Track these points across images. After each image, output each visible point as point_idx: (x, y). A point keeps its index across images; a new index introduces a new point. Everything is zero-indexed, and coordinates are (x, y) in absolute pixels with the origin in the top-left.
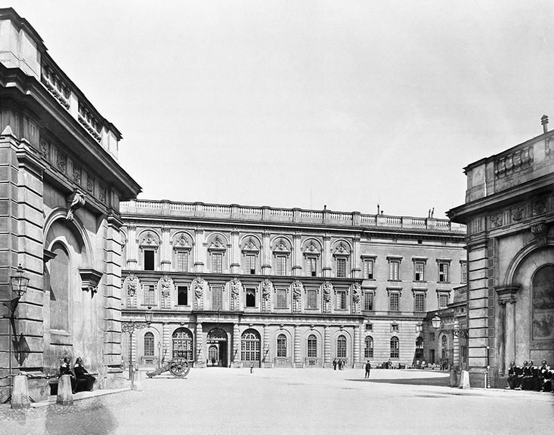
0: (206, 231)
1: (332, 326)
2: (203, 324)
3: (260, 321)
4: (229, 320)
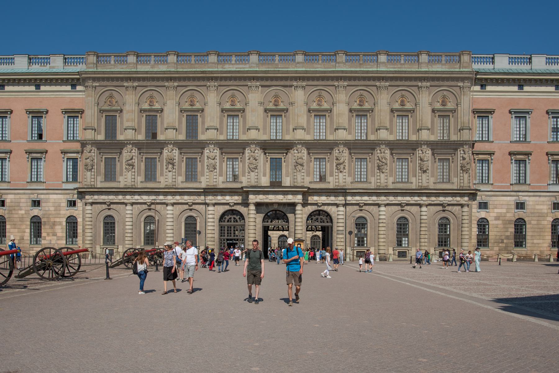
0: (262, 86)
1: (430, 205)
2: (258, 205)
3: (332, 199)
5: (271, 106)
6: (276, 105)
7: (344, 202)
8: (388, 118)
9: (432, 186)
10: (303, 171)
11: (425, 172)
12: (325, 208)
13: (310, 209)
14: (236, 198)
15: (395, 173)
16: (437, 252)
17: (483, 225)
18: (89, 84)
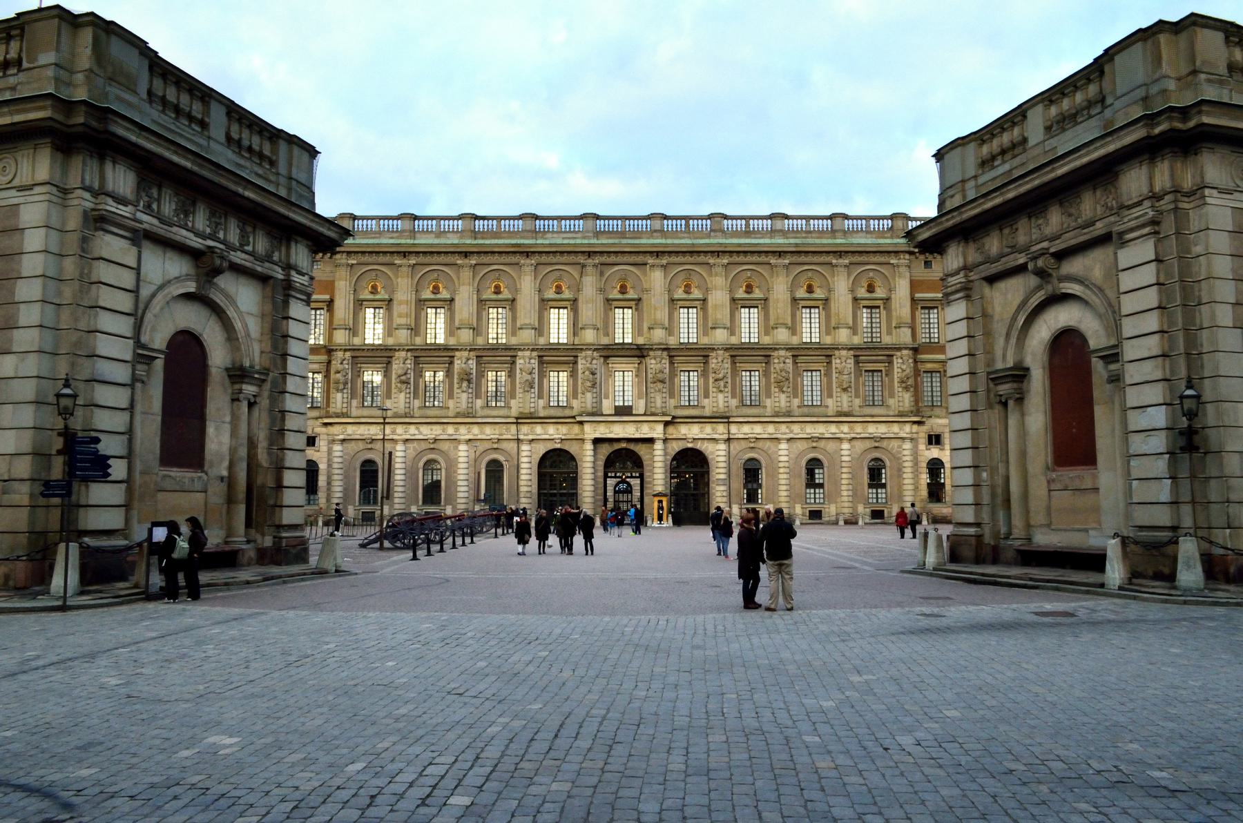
2: (597, 441)
4: (645, 431)
5: (615, 294)
7: (726, 436)
8: (789, 312)
9: (857, 410)
11: (845, 390)
12: (699, 446)
13: (676, 447)
14: (563, 429)
15: (803, 391)
16: (868, 511)
17: (935, 467)
18: (344, 261)
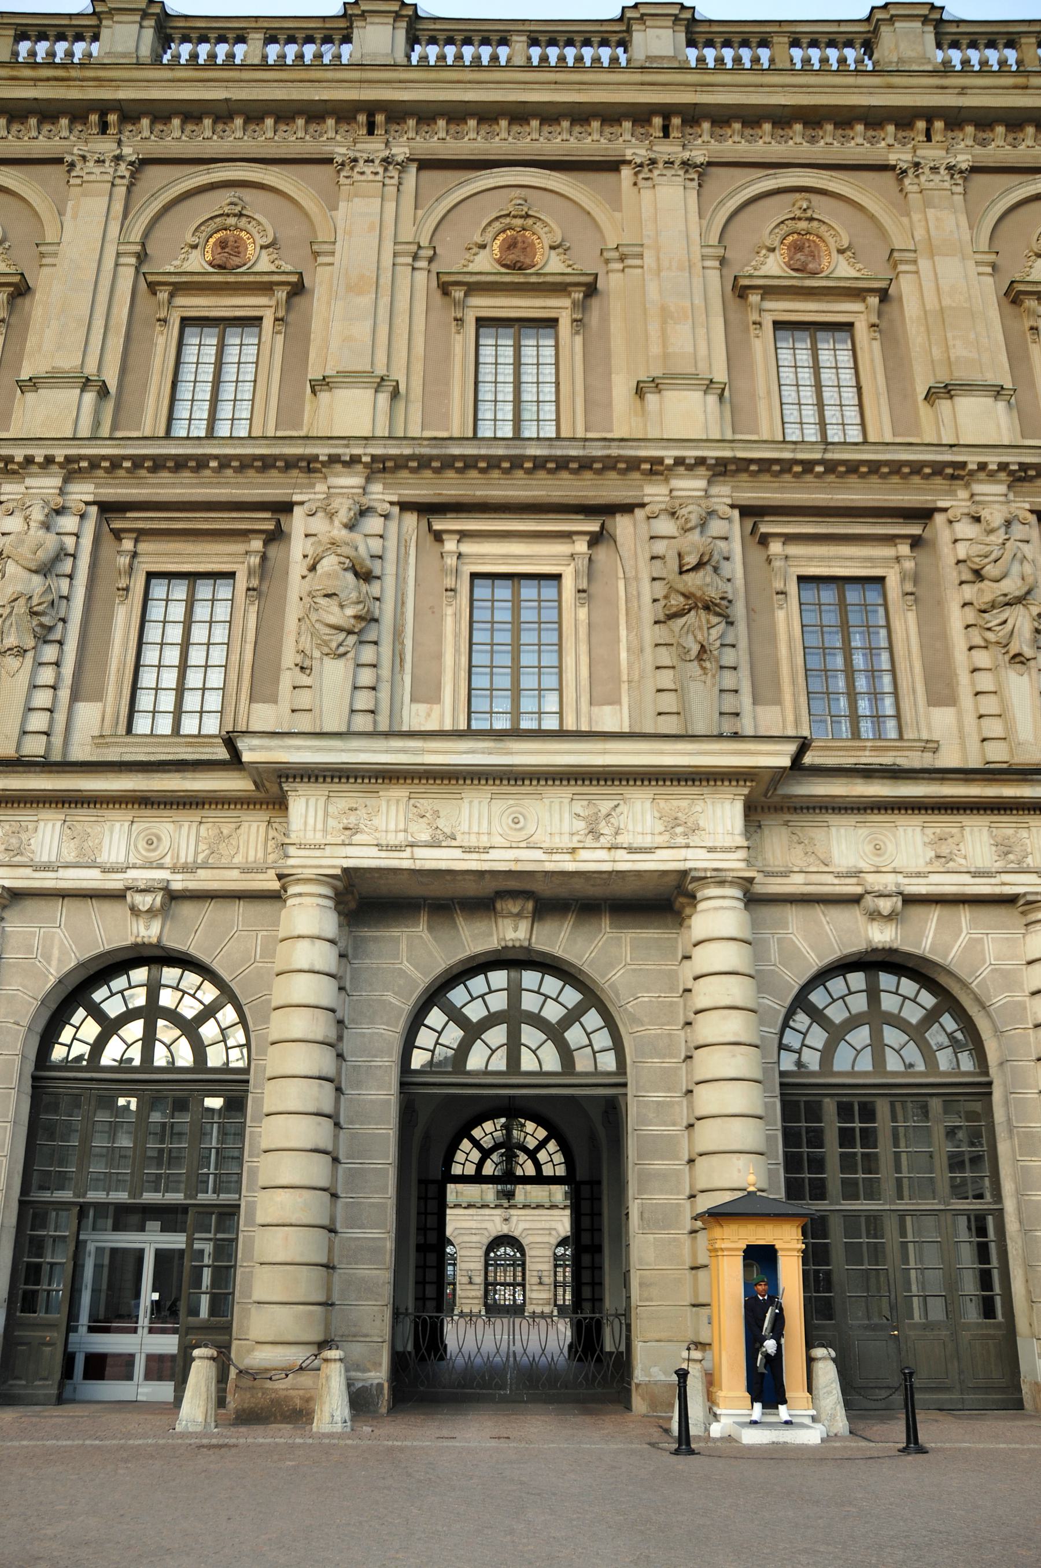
0: (426, 165)
2: (367, 902)
4: (638, 838)
6: (516, 267)
10: (729, 657)
12: (928, 936)
